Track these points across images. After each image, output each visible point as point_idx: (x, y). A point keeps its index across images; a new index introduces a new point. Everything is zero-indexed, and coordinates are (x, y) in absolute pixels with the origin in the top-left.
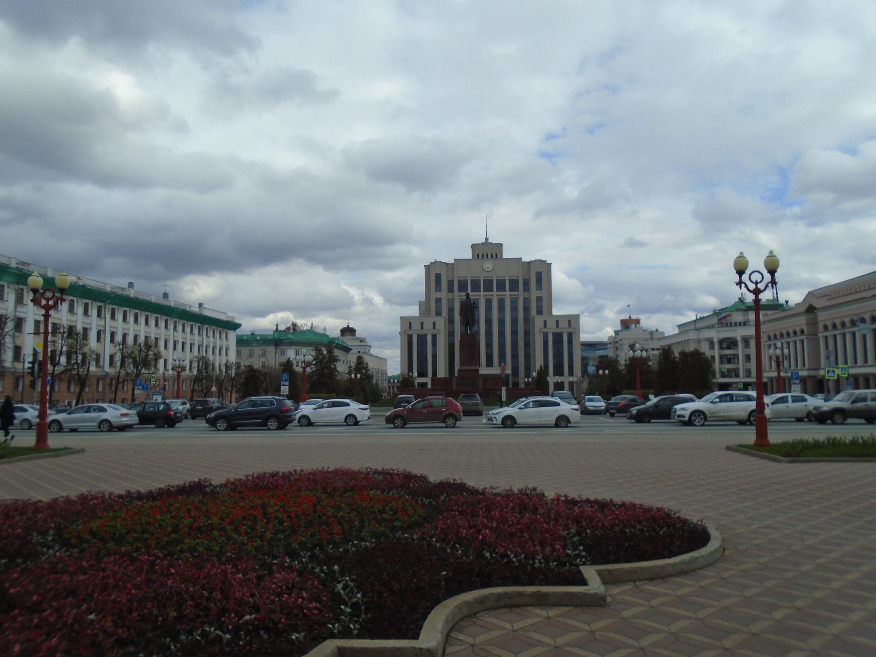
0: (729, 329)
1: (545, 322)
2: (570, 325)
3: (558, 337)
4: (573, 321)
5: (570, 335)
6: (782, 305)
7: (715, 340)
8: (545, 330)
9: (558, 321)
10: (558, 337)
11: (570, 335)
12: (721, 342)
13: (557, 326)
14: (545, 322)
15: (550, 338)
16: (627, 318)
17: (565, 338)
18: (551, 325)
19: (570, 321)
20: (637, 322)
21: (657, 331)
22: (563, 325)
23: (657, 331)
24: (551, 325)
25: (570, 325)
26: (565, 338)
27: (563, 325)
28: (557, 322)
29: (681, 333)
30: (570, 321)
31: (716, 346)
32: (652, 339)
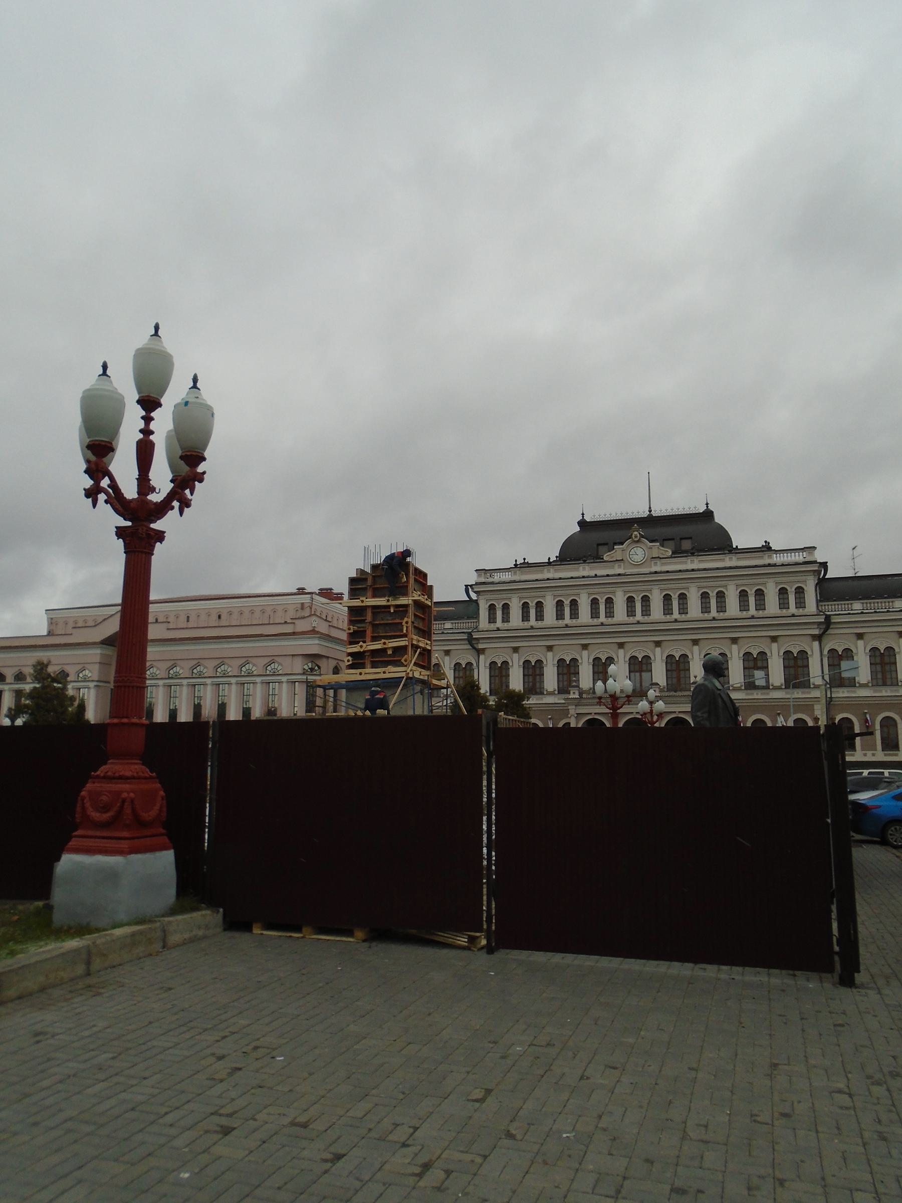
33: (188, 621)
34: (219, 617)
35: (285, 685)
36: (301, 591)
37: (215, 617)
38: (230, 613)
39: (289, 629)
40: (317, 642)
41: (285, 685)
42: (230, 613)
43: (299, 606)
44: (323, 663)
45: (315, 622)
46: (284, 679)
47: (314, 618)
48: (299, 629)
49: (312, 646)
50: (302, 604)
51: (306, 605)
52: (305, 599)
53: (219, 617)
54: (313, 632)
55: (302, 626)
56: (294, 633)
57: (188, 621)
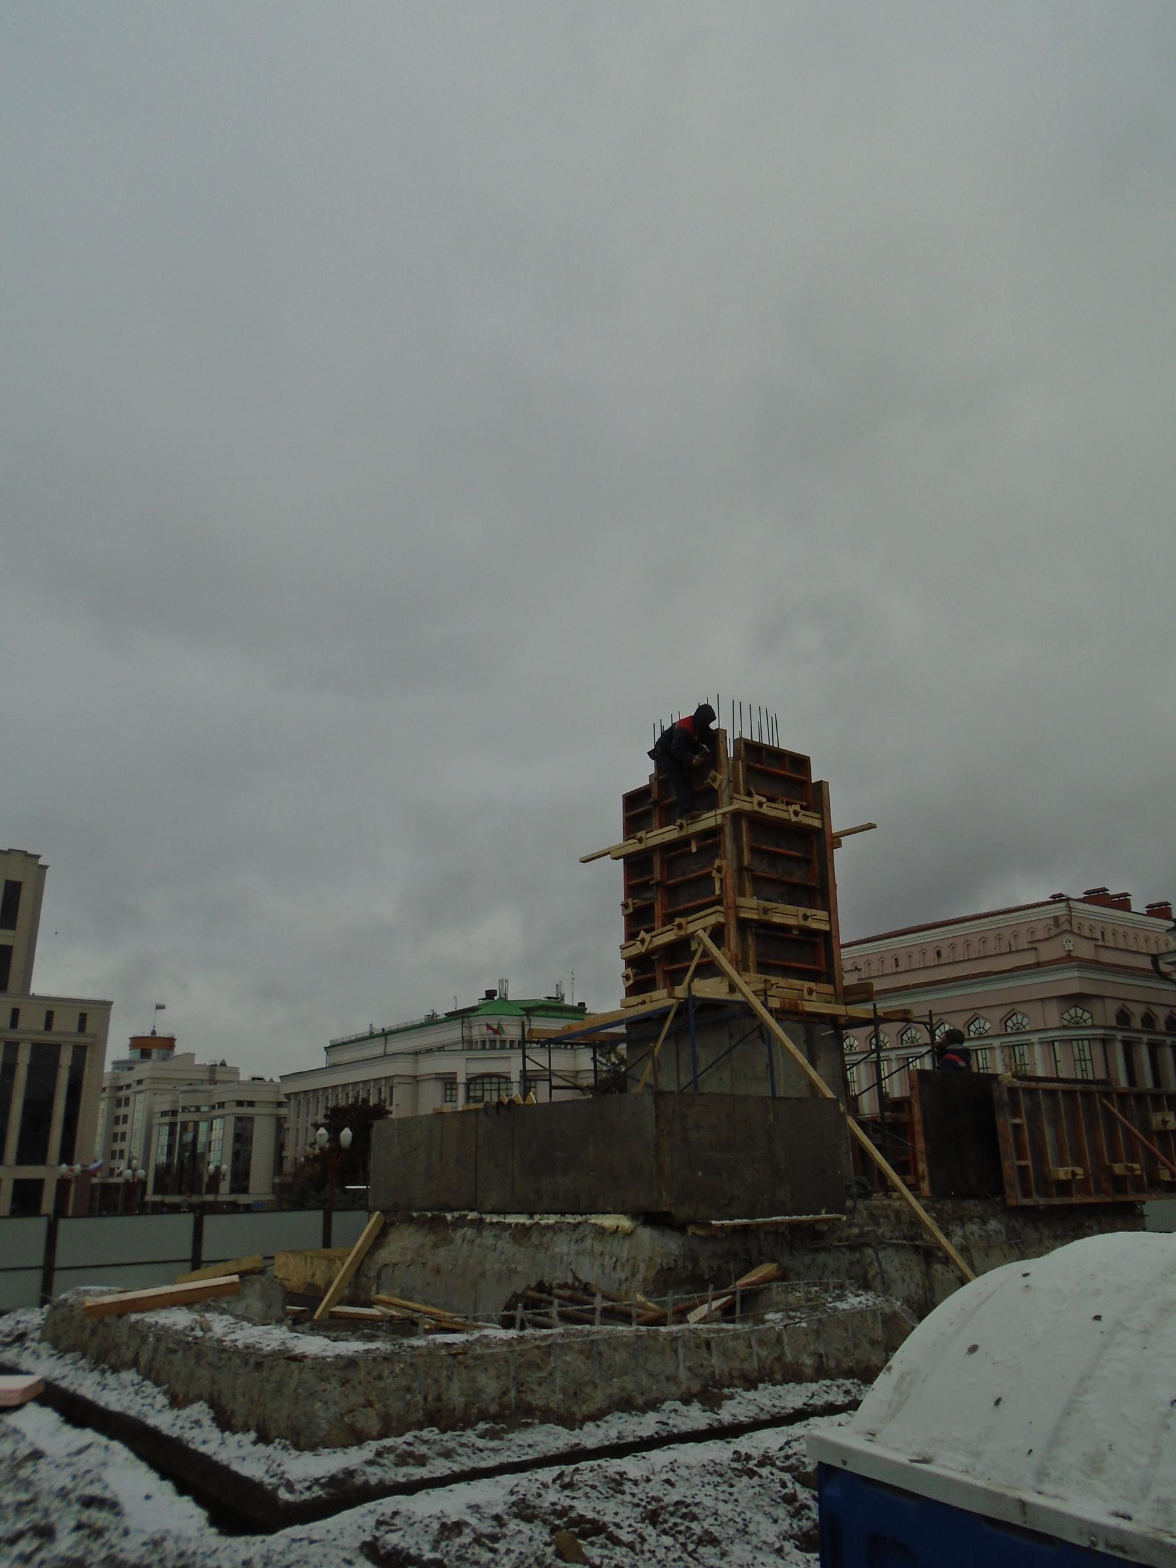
0: (503, 1053)
1: (15, 1013)
2: (82, 1027)
3: (46, 1056)
4: (90, 1016)
5: (80, 1052)
6: (571, 1009)
7: (461, 1079)
8: (12, 1035)
9: (51, 1009)
10: (46, 1056)
11: (80, 1052)
12: (471, 1081)
13: (48, 1025)
14: (15, 1013)
15: (24, 1057)
16: (148, 1034)
17: (66, 1058)
18: (32, 1022)
19: (83, 1018)
20: (169, 1043)
21: (223, 1064)
22: (65, 1024)
23: (223, 1064)
24: (32, 1022)
25: (82, 1027)
26: (66, 1058)
27: (65, 1024)
28: (50, 1016)
29: (332, 1066)
30: (83, 1018)
31: (461, 1091)
32: (213, 1081)
33: (897, 965)
34: (939, 954)
35: (1037, 1048)
36: (1058, 898)
37: (933, 955)
38: (953, 947)
39: (1029, 959)
40: (1076, 974)
41: (1037, 1048)
42: (953, 947)
43: (1051, 922)
44: (1097, 1007)
45: (1068, 943)
46: (1034, 1038)
47: (1068, 936)
48: (1045, 956)
49: (1070, 981)
50: (1056, 918)
51: (1062, 919)
52: (1060, 909)
53: (939, 954)
54: (1069, 959)
55: (1048, 952)
56: (1038, 965)
57: (897, 965)
